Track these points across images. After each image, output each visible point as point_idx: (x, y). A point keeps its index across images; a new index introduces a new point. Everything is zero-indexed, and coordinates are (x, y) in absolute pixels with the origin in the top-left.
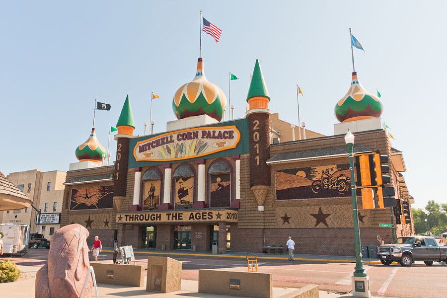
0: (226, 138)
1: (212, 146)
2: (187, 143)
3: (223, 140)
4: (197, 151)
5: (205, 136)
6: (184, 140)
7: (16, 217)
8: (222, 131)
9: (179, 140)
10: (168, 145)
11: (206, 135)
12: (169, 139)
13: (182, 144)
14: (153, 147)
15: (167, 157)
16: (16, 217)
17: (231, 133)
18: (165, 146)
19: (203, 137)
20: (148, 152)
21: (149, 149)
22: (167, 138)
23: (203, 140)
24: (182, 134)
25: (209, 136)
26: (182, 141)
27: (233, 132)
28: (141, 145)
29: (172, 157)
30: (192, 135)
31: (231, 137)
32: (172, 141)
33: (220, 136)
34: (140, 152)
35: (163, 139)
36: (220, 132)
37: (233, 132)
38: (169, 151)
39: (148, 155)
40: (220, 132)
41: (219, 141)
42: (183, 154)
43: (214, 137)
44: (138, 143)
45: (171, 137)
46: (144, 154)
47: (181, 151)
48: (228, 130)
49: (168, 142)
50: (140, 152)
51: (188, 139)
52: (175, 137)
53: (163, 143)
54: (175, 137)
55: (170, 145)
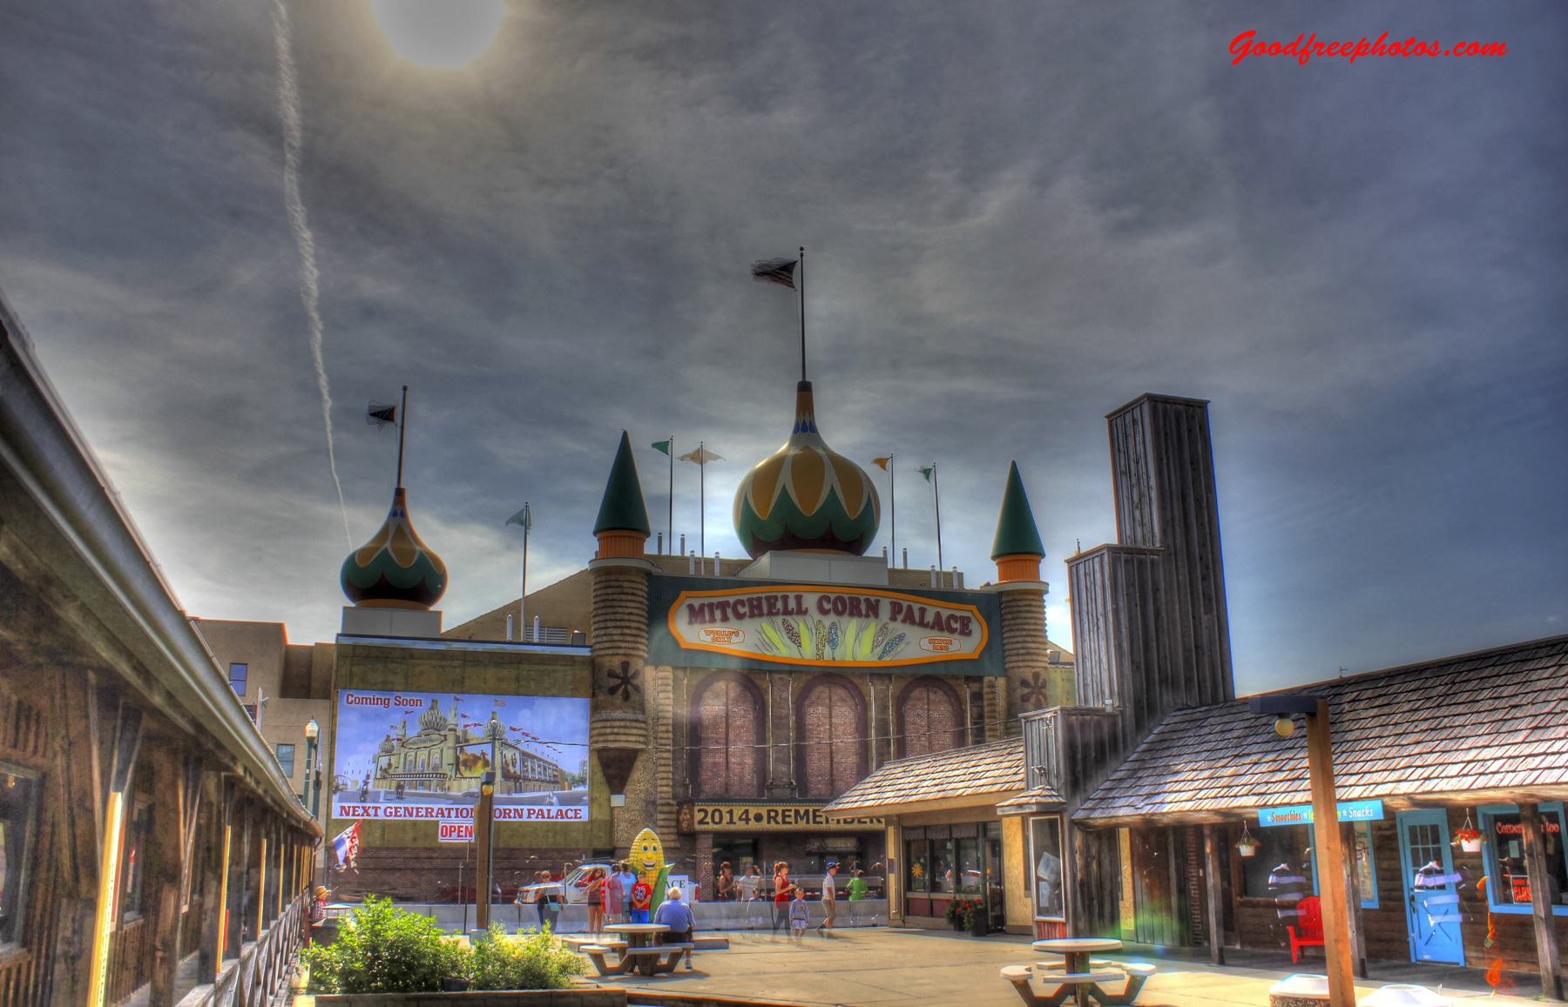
0: (953, 631)
2: (851, 626)
3: (945, 636)
4: (879, 650)
5: (900, 617)
6: (839, 613)
8: (945, 613)
10: (789, 618)
12: (792, 604)
14: (740, 616)
15: (783, 650)
17: (965, 622)
18: (779, 619)
22: (785, 599)
23: (891, 625)
24: (833, 597)
25: (909, 619)
26: (832, 618)
27: (969, 619)
30: (863, 607)
31: (965, 632)
32: (801, 611)
33: (938, 625)
35: (772, 601)
36: (938, 615)
37: (969, 619)
38: (794, 637)
40: (938, 615)
41: (935, 634)
43: (922, 624)
45: (799, 599)
46: (708, 633)
47: (833, 643)
48: (958, 614)
51: (852, 615)
52: (810, 600)
54: (810, 600)
55: (801, 626)
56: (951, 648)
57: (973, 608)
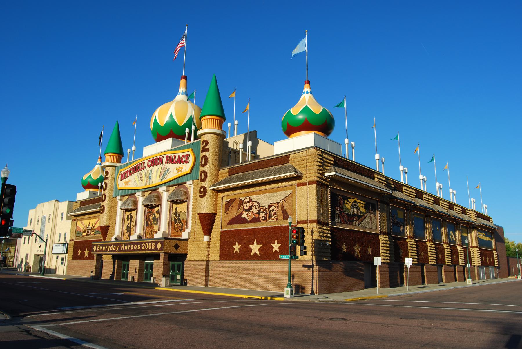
1: (174, 171)
2: (155, 168)
4: (161, 177)
7: (40, 246)
9: (149, 166)
11: (170, 160)
13: (151, 170)
14: (131, 174)
16: (40, 246)
17: (187, 156)
18: (139, 173)
19: (166, 163)
20: (127, 180)
21: (128, 177)
28: (122, 173)
29: (142, 185)
31: (187, 162)
32: (144, 168)
33: (180, 161)
34: (121, 180)
36: (179, 156)
39: (127, 183)
40: (179, 156)
42: (151, 180)
43: (175, 162)
44: (120, 170)
45: (144, 163)
49: (141, 169)
50: (121, 180)
51: (156, 165)
53: (138, 171)
55: (143, 172)
56: (183, 170)
57: (190, 150)
